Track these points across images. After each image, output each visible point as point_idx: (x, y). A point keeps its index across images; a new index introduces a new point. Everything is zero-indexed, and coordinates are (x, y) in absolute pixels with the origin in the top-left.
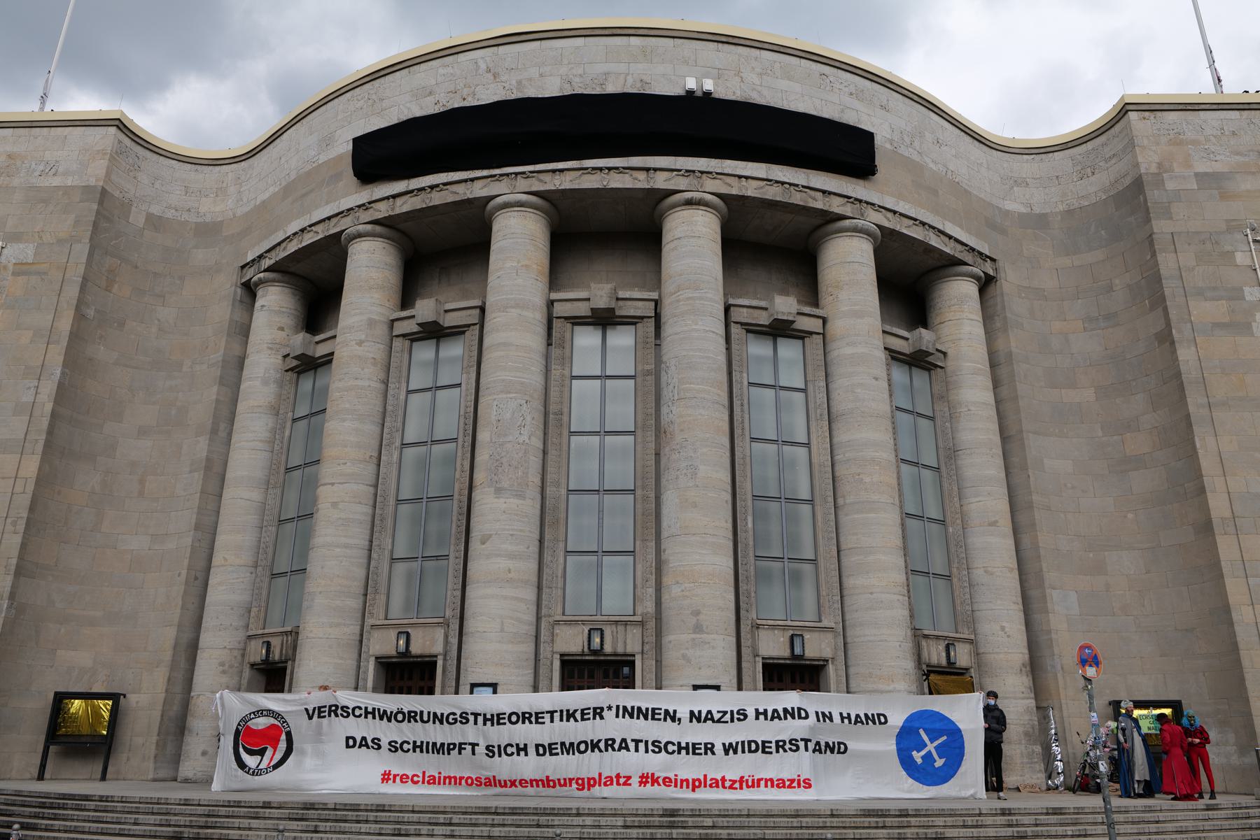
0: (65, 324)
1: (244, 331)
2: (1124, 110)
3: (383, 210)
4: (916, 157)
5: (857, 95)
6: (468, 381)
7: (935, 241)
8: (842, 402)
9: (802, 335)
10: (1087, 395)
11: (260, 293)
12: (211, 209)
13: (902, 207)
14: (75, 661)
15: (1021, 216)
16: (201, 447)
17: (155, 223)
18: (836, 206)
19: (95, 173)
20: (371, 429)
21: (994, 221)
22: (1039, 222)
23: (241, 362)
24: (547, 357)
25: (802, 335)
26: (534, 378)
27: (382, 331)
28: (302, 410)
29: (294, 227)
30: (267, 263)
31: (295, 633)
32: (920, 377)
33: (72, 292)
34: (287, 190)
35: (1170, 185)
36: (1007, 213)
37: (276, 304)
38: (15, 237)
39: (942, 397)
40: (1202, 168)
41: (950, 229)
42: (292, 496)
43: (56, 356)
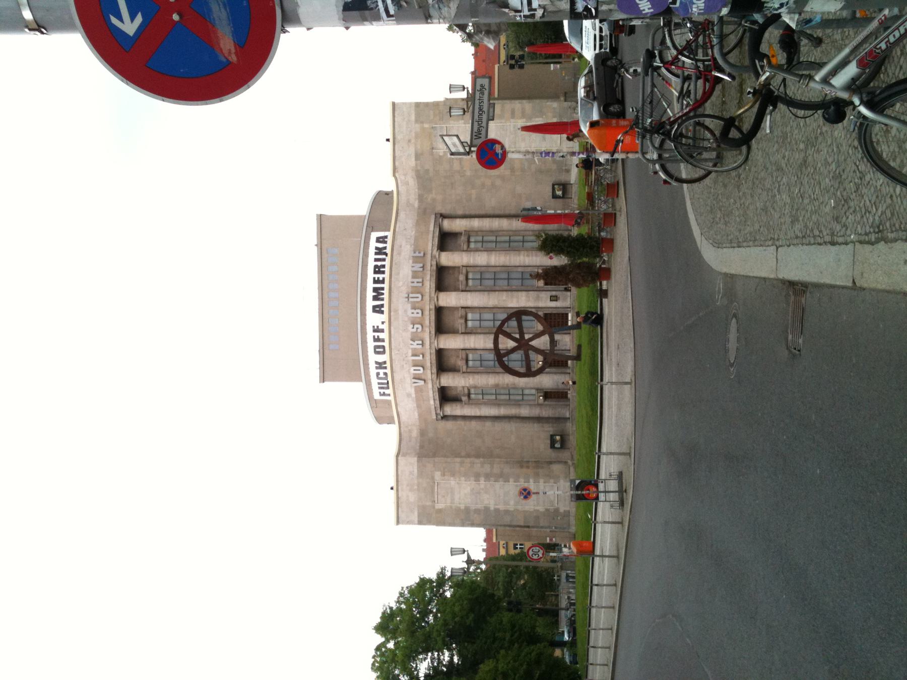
0: (458, 460)
1: (455, 418)
2: (394, 175)
3: (435, 376)
4: (413, 238)
5: (399, 254)
6: (479, 352)
7: (437, 234)
8: (484, 263)
9: (467, 273)
10: (474, 192)
11: (446, 414)
12: (415, 433)
13: (430, 245)
14: (543, 446)
15: (420, 202)
16: (488, 424)
17: (422, 447)
18: (434, 263)
19: (414, 460)
20: (491, 375)
21: (422, 214)
22: (421, 198)
23: (464, 418)
24: (475, 333)
25: (467, 273)
26: (481, 336)
27: (465, 375)
28: (480, 397)
29: (432, 402)
30: (438, 411)
31: (538, 390)
32: (472, 239)
33: (449, 460)
34: (419, 406)
35: (419, 168)
36: (419, 208)
37: (449, 410)
38: (433, 478)
39: (477, 232)
40: (413, 159)
41: (432, 228)
42: (503, 397)
43: (468, 460)
